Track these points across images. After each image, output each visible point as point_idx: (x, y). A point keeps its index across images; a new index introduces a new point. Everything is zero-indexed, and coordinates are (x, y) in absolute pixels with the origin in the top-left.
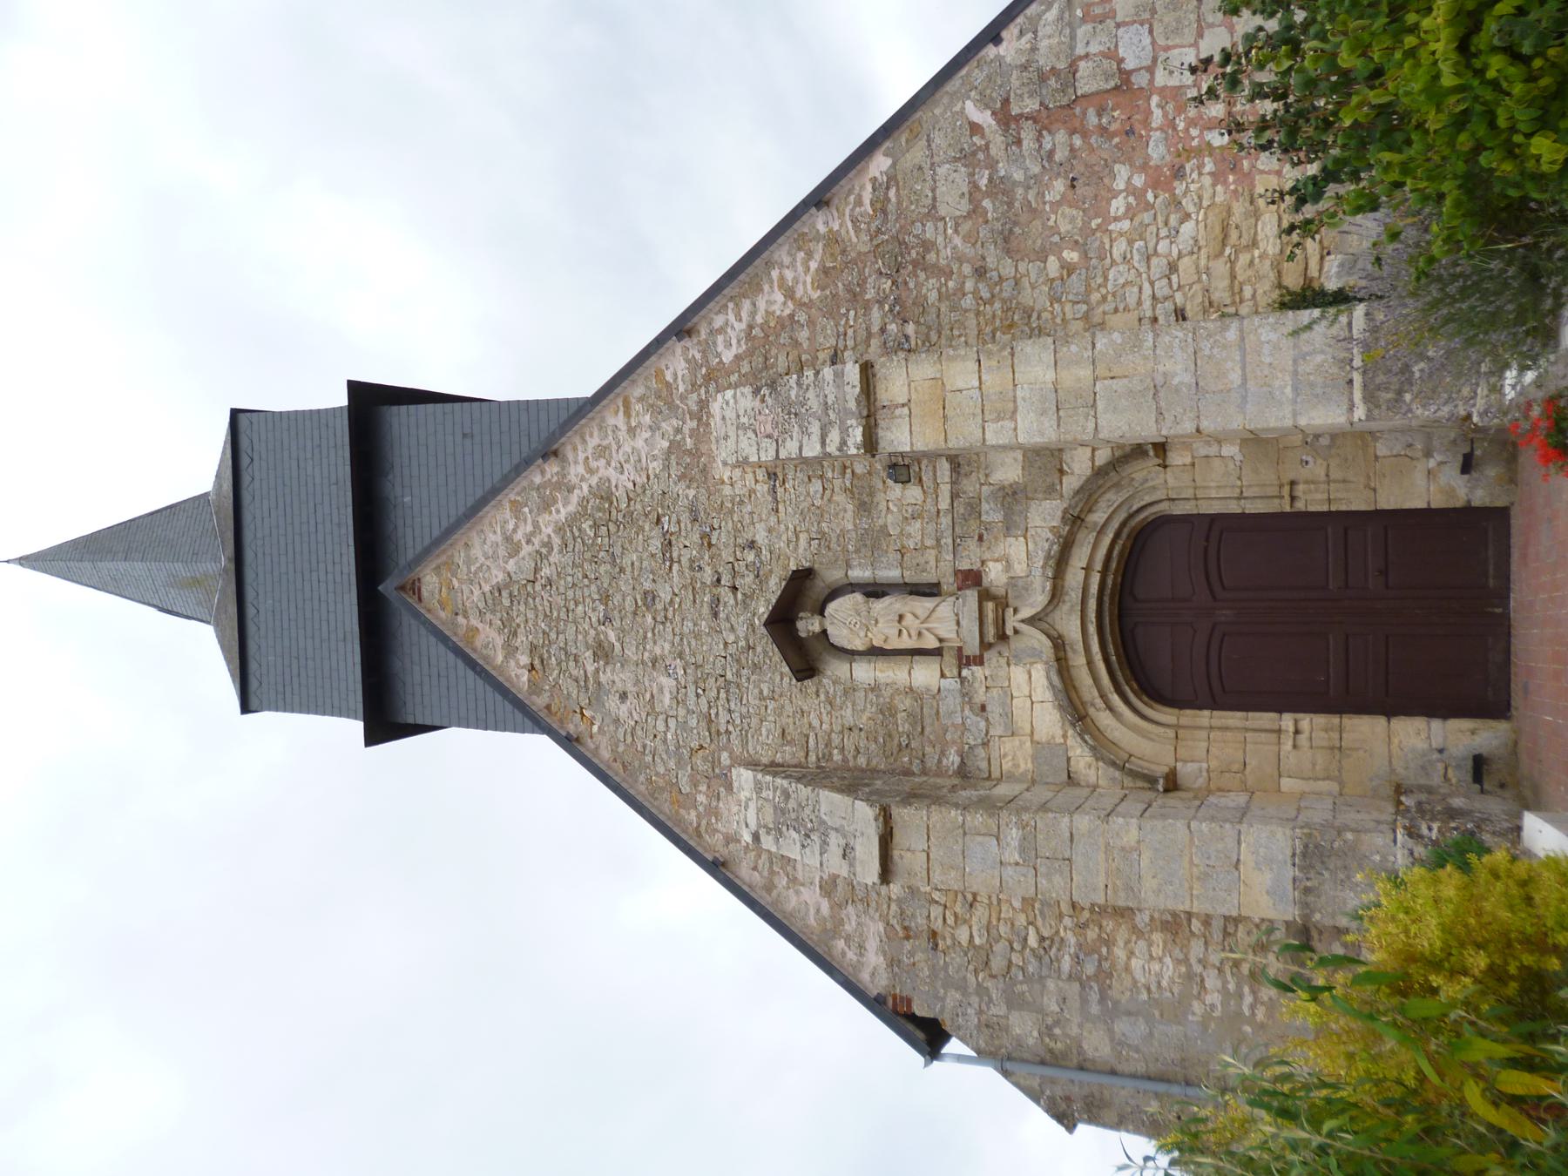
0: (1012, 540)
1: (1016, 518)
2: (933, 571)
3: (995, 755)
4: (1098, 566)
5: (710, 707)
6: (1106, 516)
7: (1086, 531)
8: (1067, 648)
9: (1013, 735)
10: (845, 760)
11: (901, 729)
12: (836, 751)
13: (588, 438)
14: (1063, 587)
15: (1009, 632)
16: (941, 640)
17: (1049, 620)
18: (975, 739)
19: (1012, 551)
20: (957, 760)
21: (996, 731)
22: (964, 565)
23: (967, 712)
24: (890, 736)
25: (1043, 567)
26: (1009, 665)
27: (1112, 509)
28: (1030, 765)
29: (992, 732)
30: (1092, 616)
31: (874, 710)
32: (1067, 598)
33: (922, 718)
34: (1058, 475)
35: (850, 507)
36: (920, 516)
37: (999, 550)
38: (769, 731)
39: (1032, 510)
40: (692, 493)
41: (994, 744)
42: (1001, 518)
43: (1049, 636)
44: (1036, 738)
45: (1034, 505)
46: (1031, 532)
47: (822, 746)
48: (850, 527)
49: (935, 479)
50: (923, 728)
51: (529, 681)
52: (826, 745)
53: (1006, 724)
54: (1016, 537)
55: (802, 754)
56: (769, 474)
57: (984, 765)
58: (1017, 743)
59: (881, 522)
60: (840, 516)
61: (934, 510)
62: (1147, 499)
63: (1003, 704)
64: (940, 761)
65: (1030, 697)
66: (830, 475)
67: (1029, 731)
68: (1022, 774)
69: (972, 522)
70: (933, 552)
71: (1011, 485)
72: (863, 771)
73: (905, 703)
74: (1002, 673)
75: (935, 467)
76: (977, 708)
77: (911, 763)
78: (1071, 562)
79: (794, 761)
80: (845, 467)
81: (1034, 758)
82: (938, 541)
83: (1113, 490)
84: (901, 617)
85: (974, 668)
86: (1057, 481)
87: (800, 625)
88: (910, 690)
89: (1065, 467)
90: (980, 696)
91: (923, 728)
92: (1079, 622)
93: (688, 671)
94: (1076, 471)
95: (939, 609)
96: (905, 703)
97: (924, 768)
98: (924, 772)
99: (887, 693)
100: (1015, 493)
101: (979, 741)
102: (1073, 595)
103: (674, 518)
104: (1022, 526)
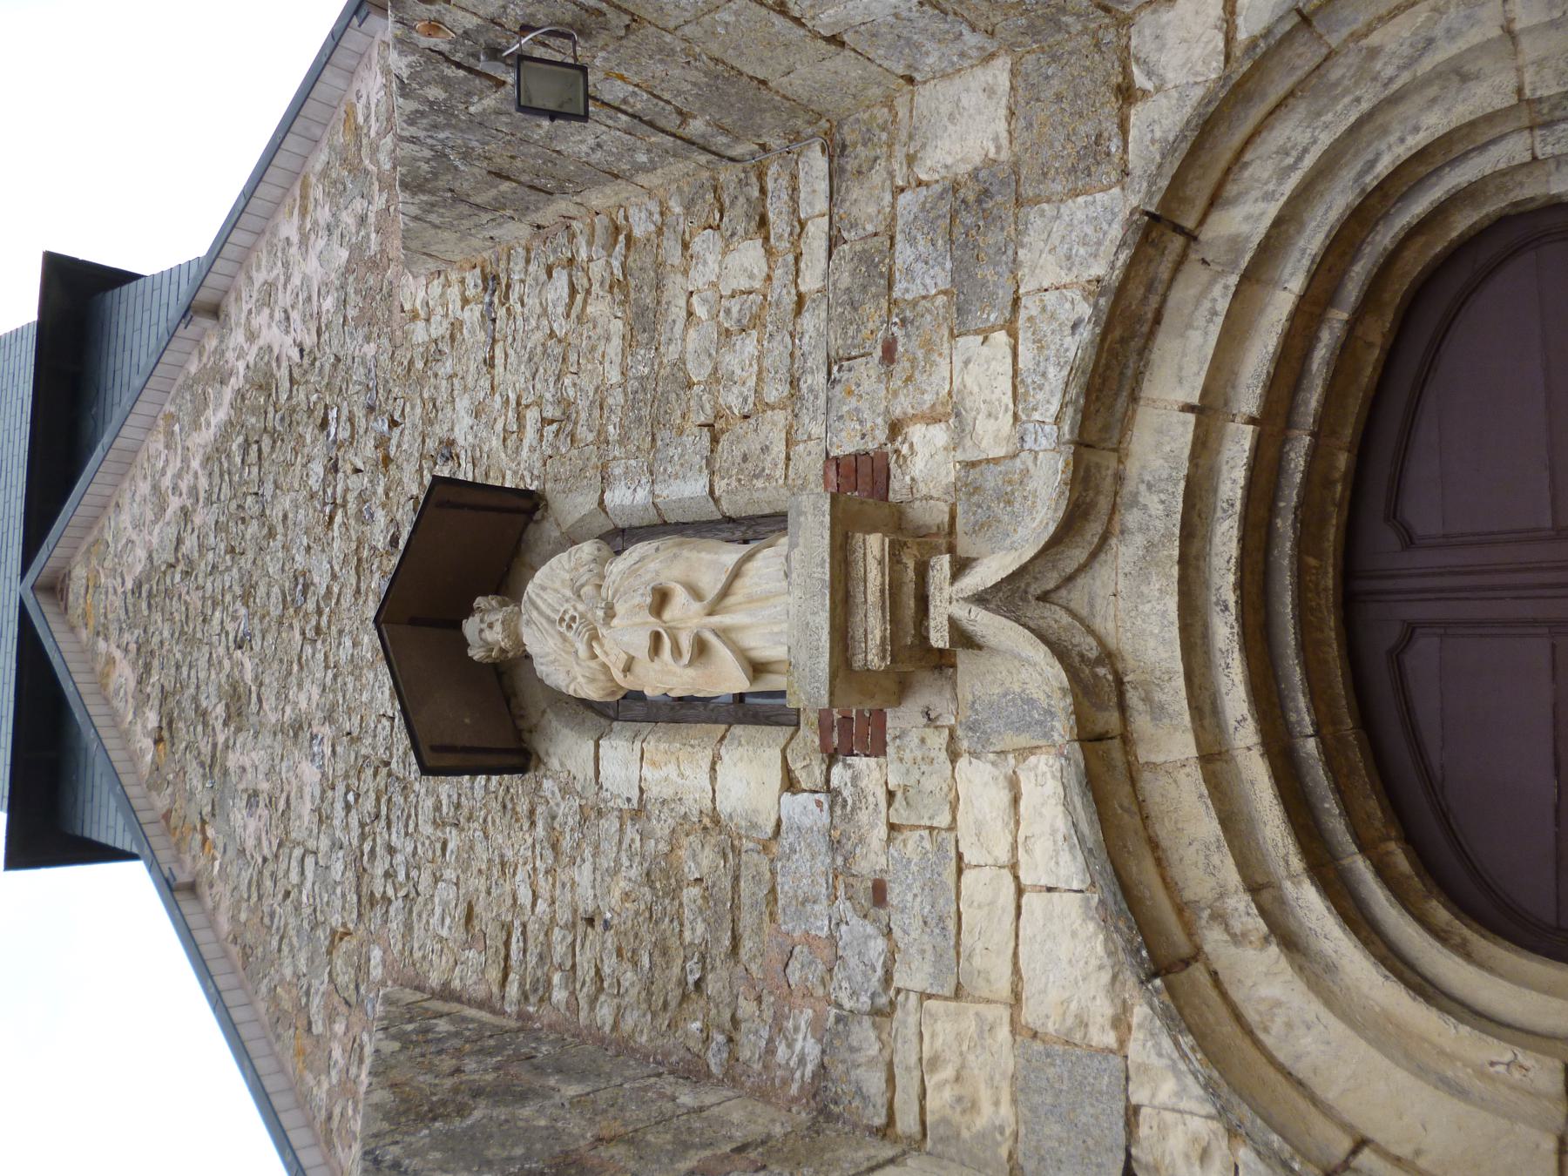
0: (971, 342)
1: (986, 272)
2: (780, 472)
3: (906, 1055)
4: (1248, 400)
5: (363, 837)
6: (1272, 210)
7: (1204, 275)
8: (1133, 698)
9: (958, 993)
10: (573, 1004)
11: (687, 935)
12: (556, 978)
13: (254, 274)
14: (1119, 478)
15: (939, 638)
16: (757, 669)
17: (1077, 596)
18: (854, 994)
19: (971, 379)
20: (812, 1049)
21: (913, 976)
22: (846, 445)
23: (843, 905)
24: (664, 953)
25: (1058, 420)
26: (954, 756)
27: (1295, 179)
28: (1006, 1110)
29: (899, 980)
30: (1223, 581)
31: (633, 873)
32: (1132, 518)
33: (735, 907)
34: (1113, 104)
35: (617, 327)
36: (756, 321)
37: (934, 386)
38: (445, 904)
39: (1033, 237)
40: (370, 349)
41: (907, 1016)
42: (944, 284)
43: (1060, 651)
44: (1029, 1016)
45: (1036, 219)
46: (1029, 307)
47: (532, 960)
48: (614, 376)
49: (795, 211)
50: (736, 940)
51: (153, 762)
52: (541, 957)
53: (939, 957)
54: (985, 334)
55: (494, 974)
56: (485, 279)
57: (874, 1082)
58: (970, 1025)
59: (672, 353)
60: (598, 355)
61: (789, 300)
62: (1435, 123)
63: (932, 887)
64: (770, 1050)
65: (1014, 867)
66: (583, 254)
67: (1003, 987)
68: (982, 1136)
69: (869, 308)
70: (780, 417)
71: (974, 175)
72: (602, 1042)
73: (699, 860)
74: (934, 782)
75: (794, 177)
76: (863, 888)
77: (707, 1040)
78: (1149, 390)
79: (480, 992)
80: (617, 230)
81: (1021, 1087)
82: (794, 383)
83: (1301, 109)
84: (661, 598)
85: (860, 762)
86: (1111, 127)
87: (470, 627)
88: (714, 822)
89: (1140, 79)
90: (872, 858)
91: (736, 940)
92: (1172, 604)
93: (339, 749)
94: (1173, 77)
95: (751, 567)
96: (699, 860)
97: (734, 1058)
98: (732, 1076)
99: (661, 827)
100: (986, 193)
101: (865, 1002)
102: (1155, 507)
103: (345, 413)
104: (1004, 296)
